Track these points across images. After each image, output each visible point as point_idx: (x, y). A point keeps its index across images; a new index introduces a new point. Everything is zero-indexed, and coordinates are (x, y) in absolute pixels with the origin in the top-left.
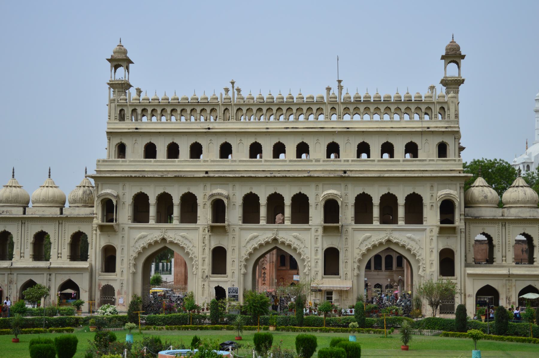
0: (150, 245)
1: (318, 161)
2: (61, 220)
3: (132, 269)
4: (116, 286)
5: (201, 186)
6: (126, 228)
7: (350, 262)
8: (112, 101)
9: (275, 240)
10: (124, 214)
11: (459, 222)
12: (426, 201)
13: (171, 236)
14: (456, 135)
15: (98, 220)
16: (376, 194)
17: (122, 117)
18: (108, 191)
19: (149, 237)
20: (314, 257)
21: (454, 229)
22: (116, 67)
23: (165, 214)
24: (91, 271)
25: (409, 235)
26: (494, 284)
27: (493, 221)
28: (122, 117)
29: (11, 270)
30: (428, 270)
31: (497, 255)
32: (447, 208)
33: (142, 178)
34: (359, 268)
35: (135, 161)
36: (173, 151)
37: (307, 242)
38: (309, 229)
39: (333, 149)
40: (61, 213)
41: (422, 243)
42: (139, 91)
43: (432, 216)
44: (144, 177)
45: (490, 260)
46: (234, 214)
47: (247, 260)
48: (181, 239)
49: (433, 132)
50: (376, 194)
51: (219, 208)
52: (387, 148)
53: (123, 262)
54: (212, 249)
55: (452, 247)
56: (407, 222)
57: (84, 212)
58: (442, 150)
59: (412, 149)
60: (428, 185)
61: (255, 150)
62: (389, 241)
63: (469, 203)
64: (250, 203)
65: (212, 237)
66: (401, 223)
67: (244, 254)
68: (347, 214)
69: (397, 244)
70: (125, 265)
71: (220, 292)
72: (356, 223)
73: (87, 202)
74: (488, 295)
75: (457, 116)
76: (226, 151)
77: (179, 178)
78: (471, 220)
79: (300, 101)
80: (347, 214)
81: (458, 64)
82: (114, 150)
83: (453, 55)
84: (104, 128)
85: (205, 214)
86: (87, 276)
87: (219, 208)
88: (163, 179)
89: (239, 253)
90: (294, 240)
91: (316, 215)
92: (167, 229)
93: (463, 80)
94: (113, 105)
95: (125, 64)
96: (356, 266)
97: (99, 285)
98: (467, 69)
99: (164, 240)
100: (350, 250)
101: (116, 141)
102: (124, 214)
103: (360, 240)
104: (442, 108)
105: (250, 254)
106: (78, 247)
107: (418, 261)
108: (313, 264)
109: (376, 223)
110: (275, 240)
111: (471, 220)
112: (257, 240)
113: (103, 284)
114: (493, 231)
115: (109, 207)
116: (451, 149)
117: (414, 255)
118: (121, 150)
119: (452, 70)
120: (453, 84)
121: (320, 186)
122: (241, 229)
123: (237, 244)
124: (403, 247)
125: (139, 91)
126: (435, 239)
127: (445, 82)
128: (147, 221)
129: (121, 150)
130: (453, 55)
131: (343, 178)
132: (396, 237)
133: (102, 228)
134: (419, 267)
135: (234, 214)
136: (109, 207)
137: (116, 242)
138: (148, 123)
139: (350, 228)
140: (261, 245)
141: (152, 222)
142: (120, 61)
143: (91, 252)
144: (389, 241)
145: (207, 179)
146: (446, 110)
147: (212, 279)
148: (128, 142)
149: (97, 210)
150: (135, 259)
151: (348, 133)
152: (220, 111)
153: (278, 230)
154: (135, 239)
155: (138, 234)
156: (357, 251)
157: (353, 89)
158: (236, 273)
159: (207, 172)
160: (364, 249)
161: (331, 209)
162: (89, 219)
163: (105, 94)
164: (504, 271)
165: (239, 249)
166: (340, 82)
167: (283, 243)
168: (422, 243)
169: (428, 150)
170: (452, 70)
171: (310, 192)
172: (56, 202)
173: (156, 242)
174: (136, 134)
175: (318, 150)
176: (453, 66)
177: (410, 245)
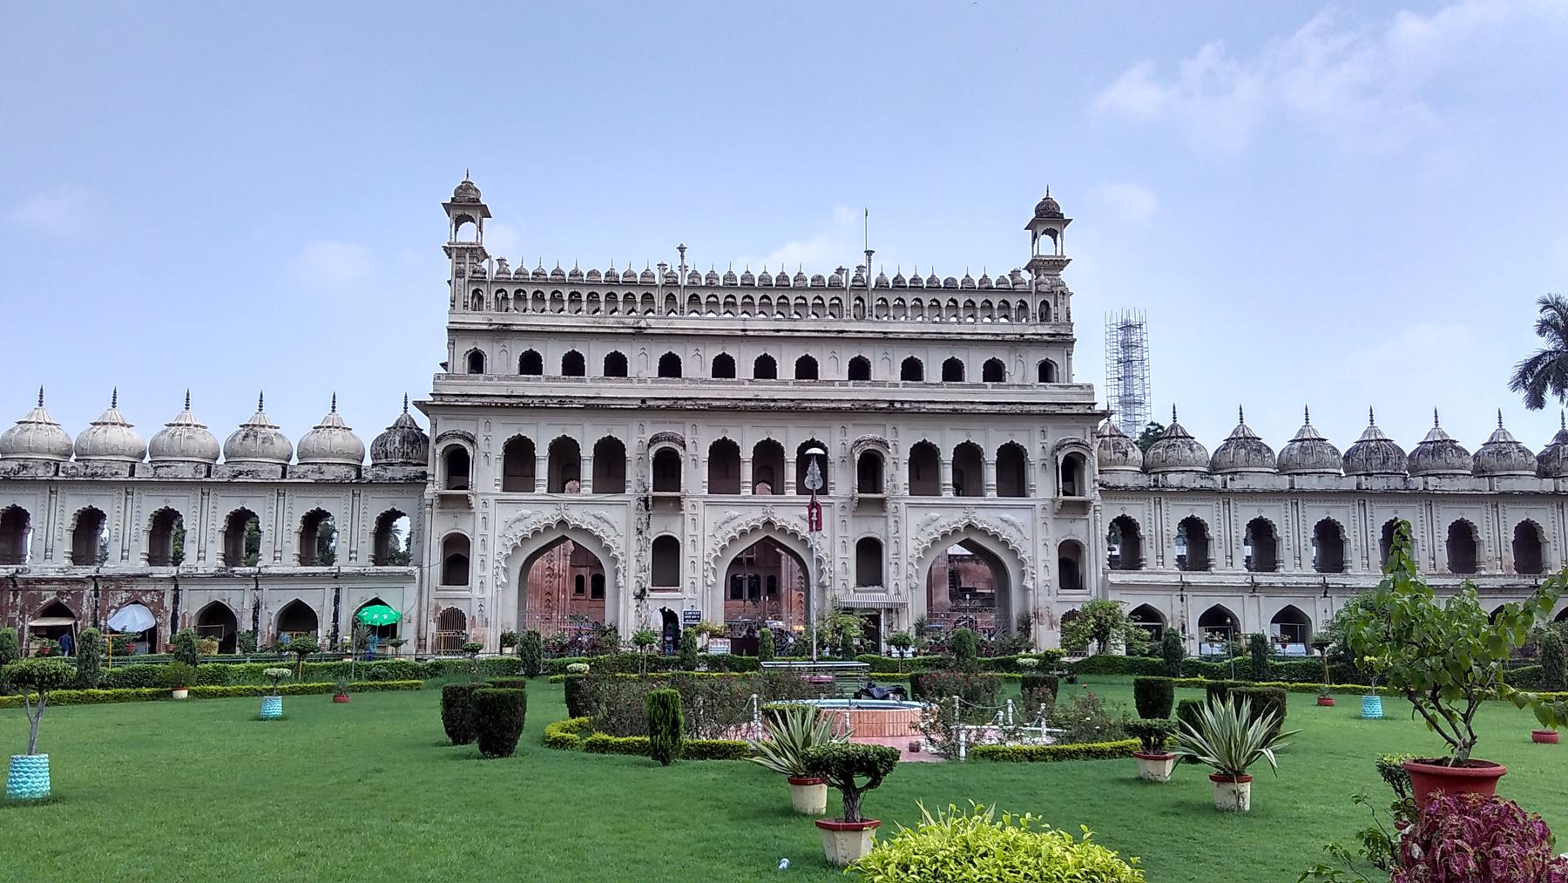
0: (536, 532)
1: (842, 383)
5: (635, 425)
6: (491, 502)
7: (903, 563)
8: (459, 274)
9: (769, 524)
10: (487, 473)
11: (1091, 492)
13: (576, 516)
16: (947, 443)
19: (534, 519)
20: (839, 552)
21: (1084, 506)
22: (459, 221)
25: (1006, 515)
26: (1155, 602)
27: (1140, 492)
29: (257, 579)
30: (1042, 577)
32: (1071, 469)
40: (359, 476)
41: (1027, 528)
43: (1043, 484)
44: (526, 407)
48: (594, 521)
49: (1030, 342)
50: (947, 443)
55: (1081, 538)
58: (1046, 371)
59: (994, 372)
60: (1037, 428)
61: (724, 368)
62: (970, 526)
64: (723, 457)
66: (992, 494)
67: (710, 546)
69: (984, 532)
70: (489, 573)
71: (669, 617)
77: (594, 409)
78: (1108, 491)
79: (800, 283)
81: (1053, 234)
82: (461, 365)
83: (1048, 218)
85: (639, 474)
87: (667, 467)
95: (477, 215)
96: (911, 570)
97: (437, 608)
98: (1071, 243)
99: (562, 523)
103: (917, 528)
104: (1045, 303)
107: (1022, 562)
108: (838, 567)
109: (948, 495)
110: (769, 524)
112: (734, 523)
117: (1014, 552)
118: (476, 362)
119: (1046, 246)
121: (850, 428)
123: (699, 532)
124: (995, 536)
127: (1036, 265)
129: (476, 362)
130: (1048, 218)
131: (893, 411)
134: (1023, 574)
136: (458, 464)
139: (903, 502)
140: (743, 533)
141: (541, 489)
142: (466, 206)
144: (970, 526)
145: (645, 409)
146: (1052, 305)
147: (654, 595)
149: (437, 469)
151: (885, 339)
152: (659, 298)
154: (500, 523)
155: (511, 513)
156: (912, 544)
157: (886, 267)
158: (699, 584)
159: (644, 401)
160: (926, 541)
161: (870, 468)
163: (447, 266)
164: (1174, 579)
166: (869, 253)
167: (783, 530)
168: (1027, 528)
169: (1021, 370)
170: (1046, 246)
172: (349, 456)
173: (548, 528)
174: (503, 332)
176: (1045, 240)
177: (1007, 533)
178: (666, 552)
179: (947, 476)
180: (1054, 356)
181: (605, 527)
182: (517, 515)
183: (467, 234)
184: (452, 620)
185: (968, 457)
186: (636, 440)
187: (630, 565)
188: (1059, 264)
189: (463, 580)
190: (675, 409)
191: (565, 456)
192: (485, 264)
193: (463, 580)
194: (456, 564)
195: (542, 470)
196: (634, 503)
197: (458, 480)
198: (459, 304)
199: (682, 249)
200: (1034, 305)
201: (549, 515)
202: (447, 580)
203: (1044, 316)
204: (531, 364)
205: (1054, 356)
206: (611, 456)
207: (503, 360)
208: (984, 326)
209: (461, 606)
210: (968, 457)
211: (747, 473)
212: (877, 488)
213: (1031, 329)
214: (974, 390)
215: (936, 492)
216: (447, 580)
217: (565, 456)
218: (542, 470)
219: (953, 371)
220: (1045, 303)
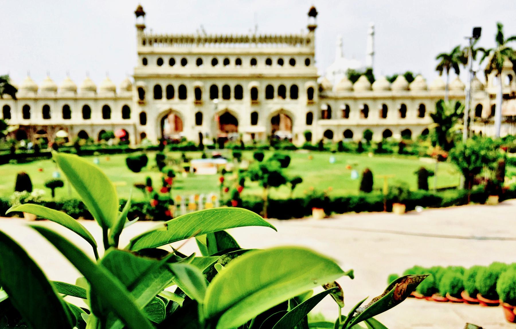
2: (116, 99)
4: (147, 133)
10: (149, 95)
14: (313, 55)
18: (141, 84)
23: (170, 96)
26: (332, 129)
31: (333, 114)
32: (310, 92)
33: (158, 76)
36: (172, 62)
37: (242, 109)
42: (151, 30)
43: (303, 96)
45: (329, 117)
46: (206, 95)
52: (281, 62)
57: (127, 94)
58: (307, 62)
63: (321, 89)
68: (262, 95)
73: (129, 88)
74: (329, 134)
76: (199, 62)
77: (177, 77)
78: (322, 97)
80: (262, 95)
82: (140, 62)
83: (313, 13)
88: (169, 77)
101: (142, 57)
102: (149, 95)
106: (126, 112)
111: (322, 97)
114: (332, 103)
115: (141, 92)
116: (311, 62)
118: (145, 62)
119: (312, 21)
120: (312, 28)
125: (151, 30)
130: (313, 13)
131: (259, 77)
135: (206, 95)
137: (147, 110)
138: (159, 48)
142: (140, 12)
148: (149, 58)
149: (135, 94)
161: (254, 92)
162: (130, 99)
163: (135, 31)
168: (298, 108)
171: (243, 84)
175: (246, 62)
176: (312, 18)
183: (141, 20)
184: (143, 135)
187: (189, 119)
190: (199, 78)
191: (170, 90)
207: (152, 61)
217: (170, 90)
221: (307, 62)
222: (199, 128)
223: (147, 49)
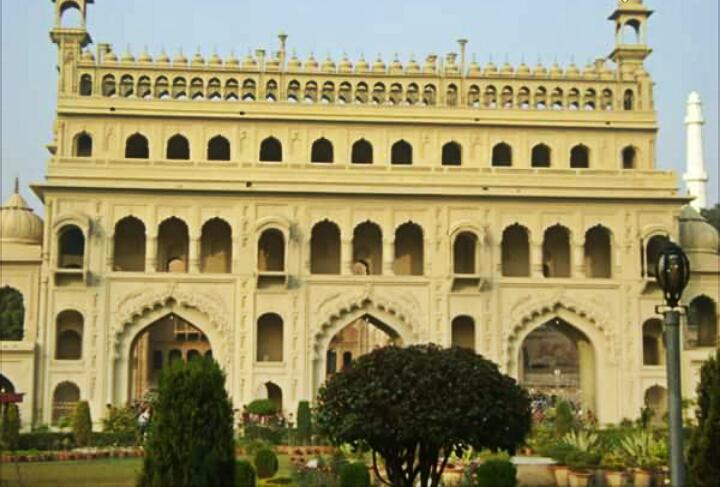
3: (112, 354)
8: (68, 60)
12: (618, 239)
13: (183, 293)
15: (50, 268)
17: (85, 87)
24: (37, 352)
28: (85, 87)
34: (510, 350)
35: (108, 159)
38: (426, 284)
39: (452, 154)
46: (296, 259)
47: (319, 337)
51: (272, 244)
53: (96, 339)
54: (258, 316)
56: (546, 272)
58: (629, 156)
61: (322, 152)
65: (258, 297)
72: (505, 274)
75: (651, 104)
76: (271, 150)
81: (635, 24)
82: (69, 146)
84: (51, 107)
86: (29, 361)
89: (307, 325)
90: (402, 303)
91: (438, 257)
92: (178, 281)
93: (650, 51)
94: (69, 67)
96: (505, 345)
99: (170, 301)
100: (494, 319)
101: (76, 128)
104: (629, 92)
105: (325, 327)
109: (537, 276)
113: (62, 379)
115: (72, 241)
116: (641, 159)
119: (628, 38)
122: (309, 283)
126: (634, 301)
127: (617, 55)
128: (141, 268)
129: (84, 144)
132: (570, 297)
133: (60, 279)
136: (72, 241)
141: (150, 268)
143: (28, 326)
150: (120, 335)
153: (374, 284)
154: (116, 301)
159: (249, 184)
160: (518, 321)
161: (464, 247)
165: (307, 318)
166: (463, 42)
169: (605, 153)
170: (628, 38)
171: (425, 217)
178: (270, 326)
179: (536, 256)
180: (640, 143)
181: (214, 305)
182: (126, 292)
185: (557, 238)
186: (246, 222)
188: (641, 54)
189: (76, 354)
192: (92, 48)
193: (76, 354)
194: (69, 336)
195: (151, 249)
196: (239, 283)
197: (68, 259)
198: (68, 88)
199: (283, 37)
200: (619, 95)
201: (160, 292)
202: (61, 354)
203: (628, 105)
204: (137, 147)
205: (640, 143)
206: (217, 234)
207: (110, 141)
208: (568, 115)
209: (74, 379)
210: (557, 238)
211: (346, 252)
212: (470, 268)
213: (618, 117)
214: (560, 176)
215: (526, 273)
216: (61, 354)
218: (151, 249)
219: (541, 156)
220: (629, 92)
221: (629, 156)
222: (271, 372)
223: (97, 102)
